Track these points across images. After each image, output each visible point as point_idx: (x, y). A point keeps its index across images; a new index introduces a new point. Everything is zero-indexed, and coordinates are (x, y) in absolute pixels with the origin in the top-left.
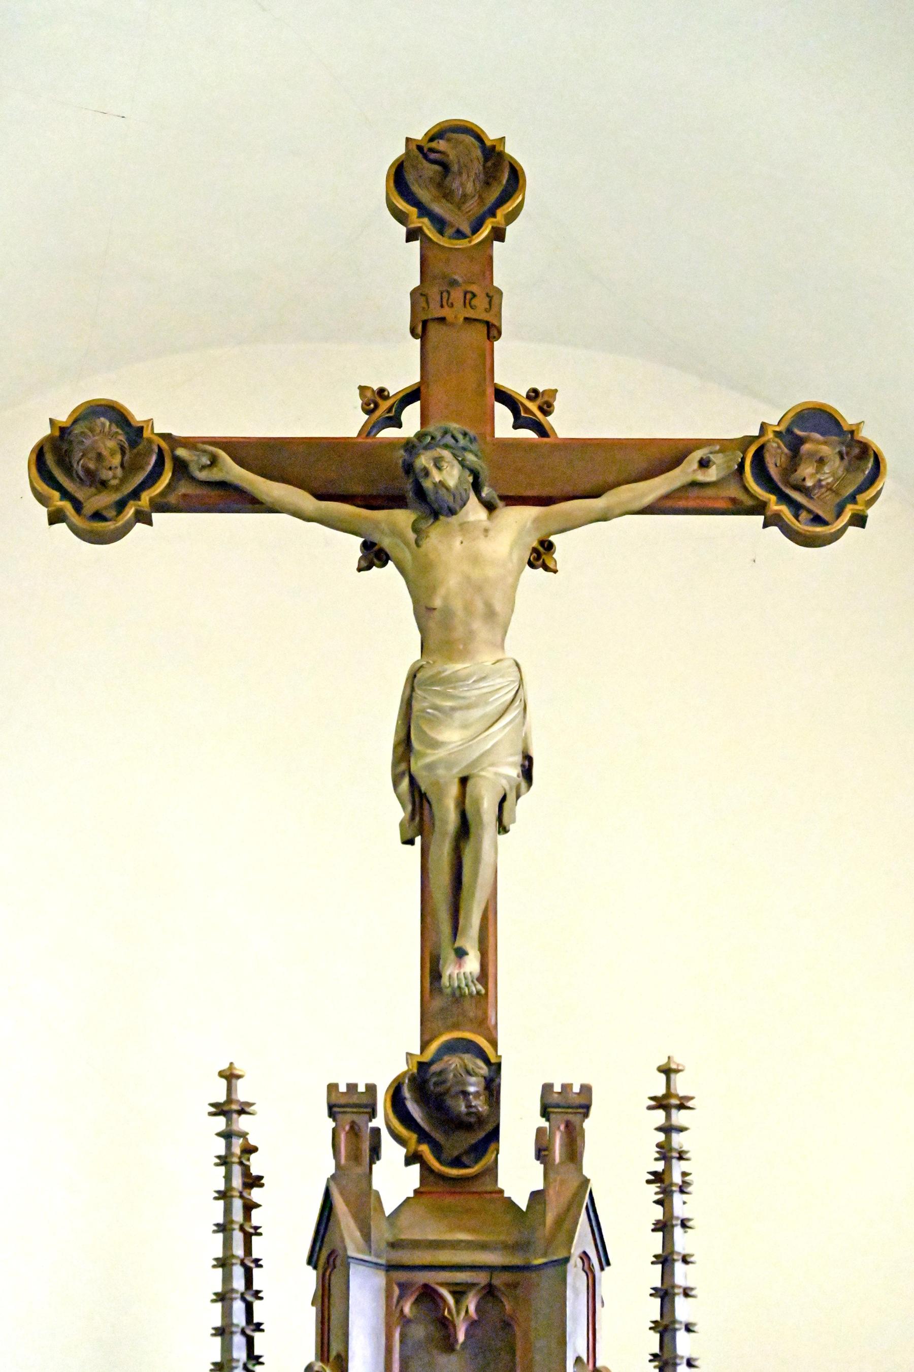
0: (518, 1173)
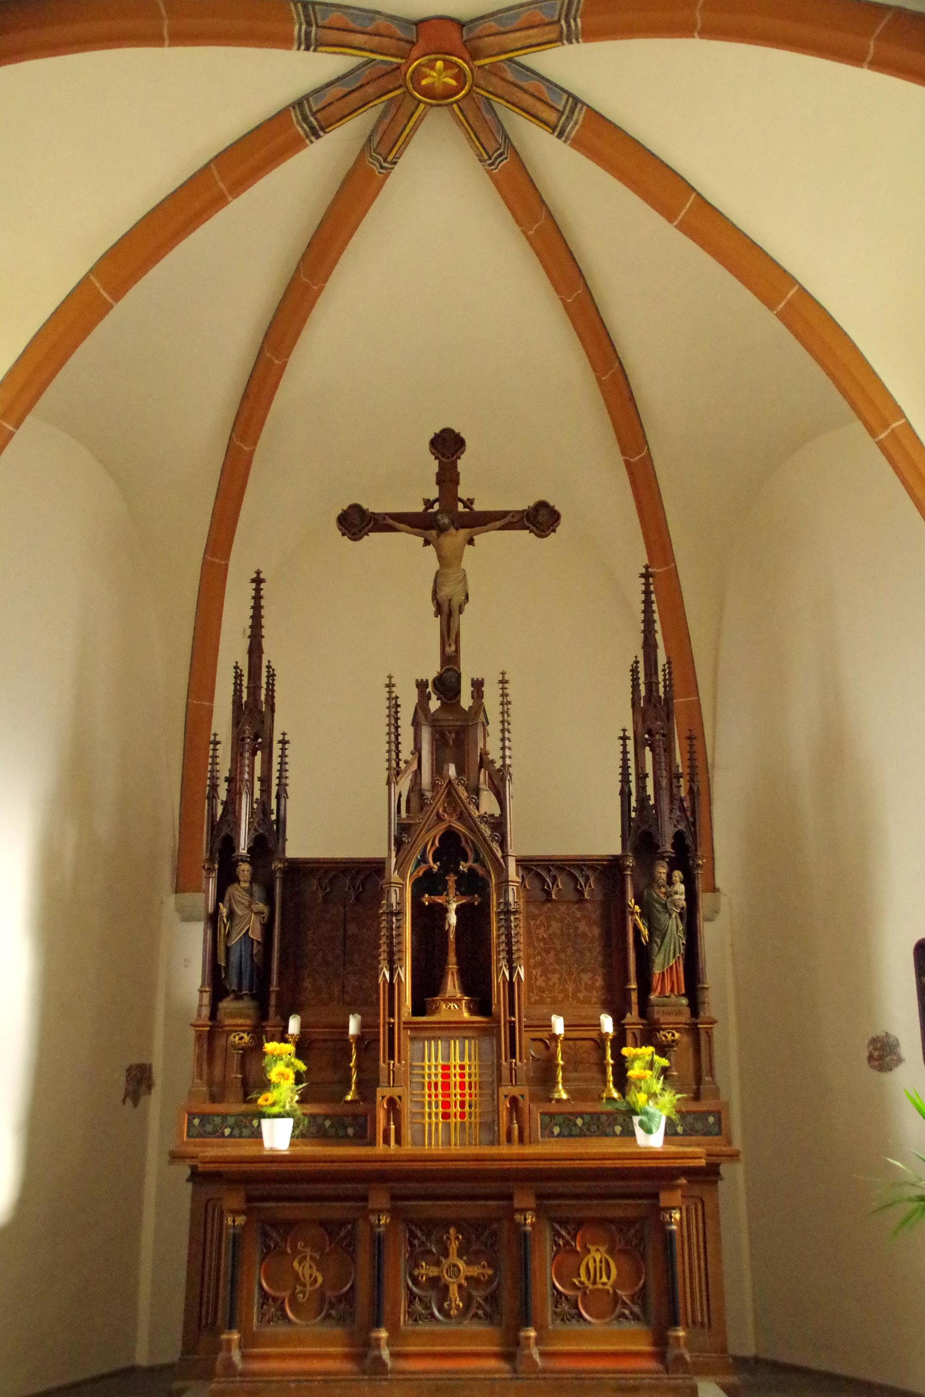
0: (466, 701)
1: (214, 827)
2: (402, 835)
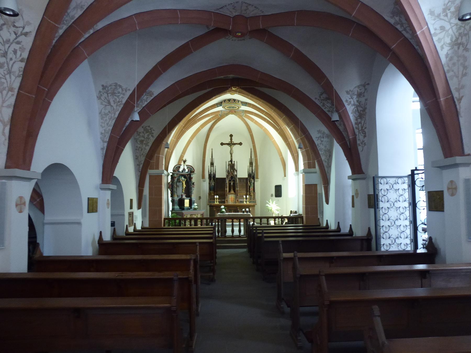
0: (233, 163)
2: (227, 176)
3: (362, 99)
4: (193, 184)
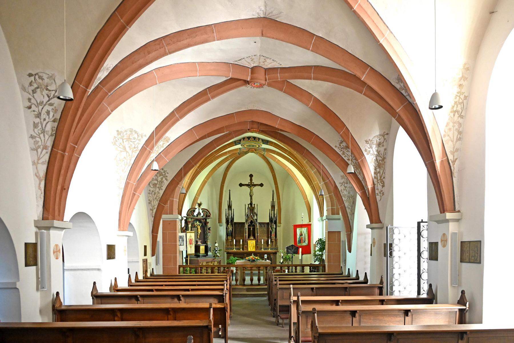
0: (253, 206)
1: (226, 219)
2: (247, 221)
3: (382, 149)
4: (209, 229)
